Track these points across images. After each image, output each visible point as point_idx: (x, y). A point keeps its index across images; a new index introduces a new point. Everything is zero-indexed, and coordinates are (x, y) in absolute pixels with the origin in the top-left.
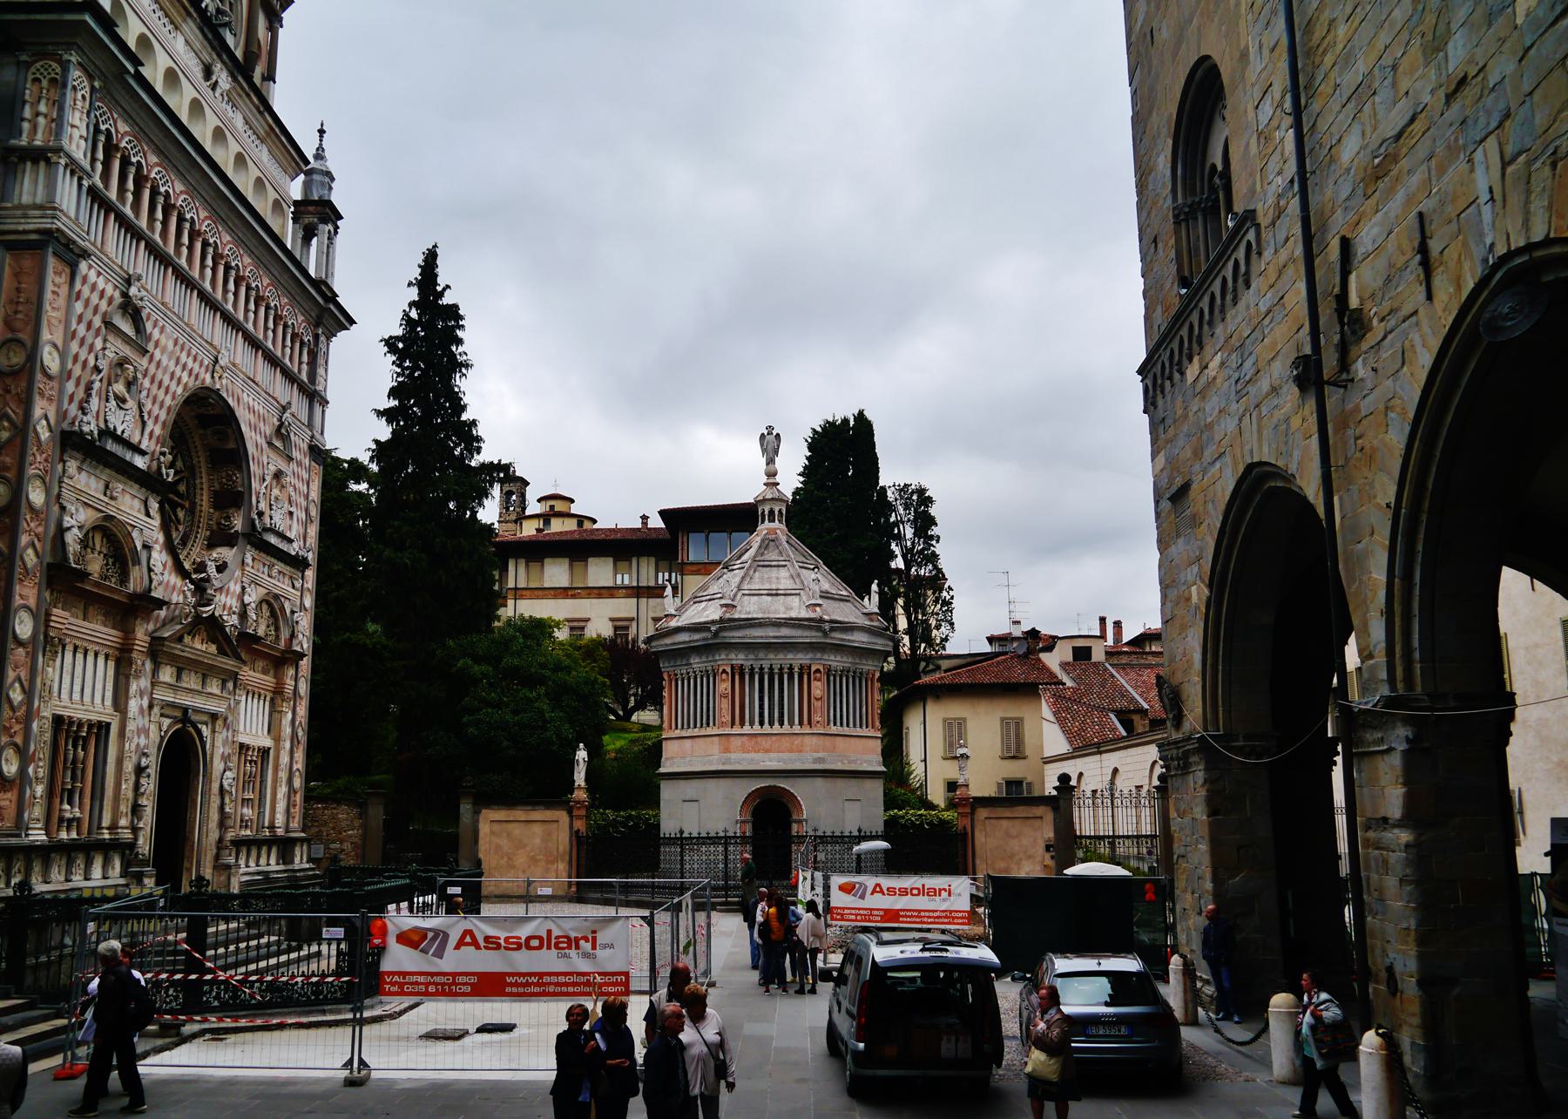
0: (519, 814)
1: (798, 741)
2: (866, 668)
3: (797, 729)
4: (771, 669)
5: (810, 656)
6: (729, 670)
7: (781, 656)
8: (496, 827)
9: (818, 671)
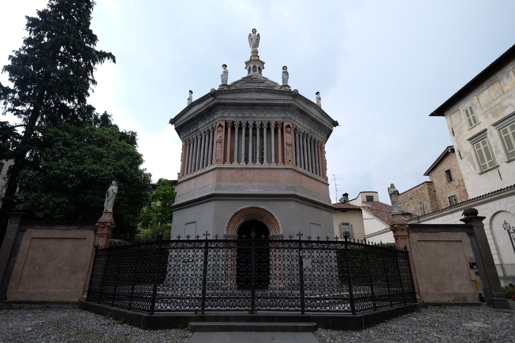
0: (56, 232)
1: (274, 173)
2: (317, 138)
3: (273, 165)
4: (254, 125)
5: (283, 115)
6: (223, 124)
7: (261, 115)
8: (35, 243)
9: (288, 126)
